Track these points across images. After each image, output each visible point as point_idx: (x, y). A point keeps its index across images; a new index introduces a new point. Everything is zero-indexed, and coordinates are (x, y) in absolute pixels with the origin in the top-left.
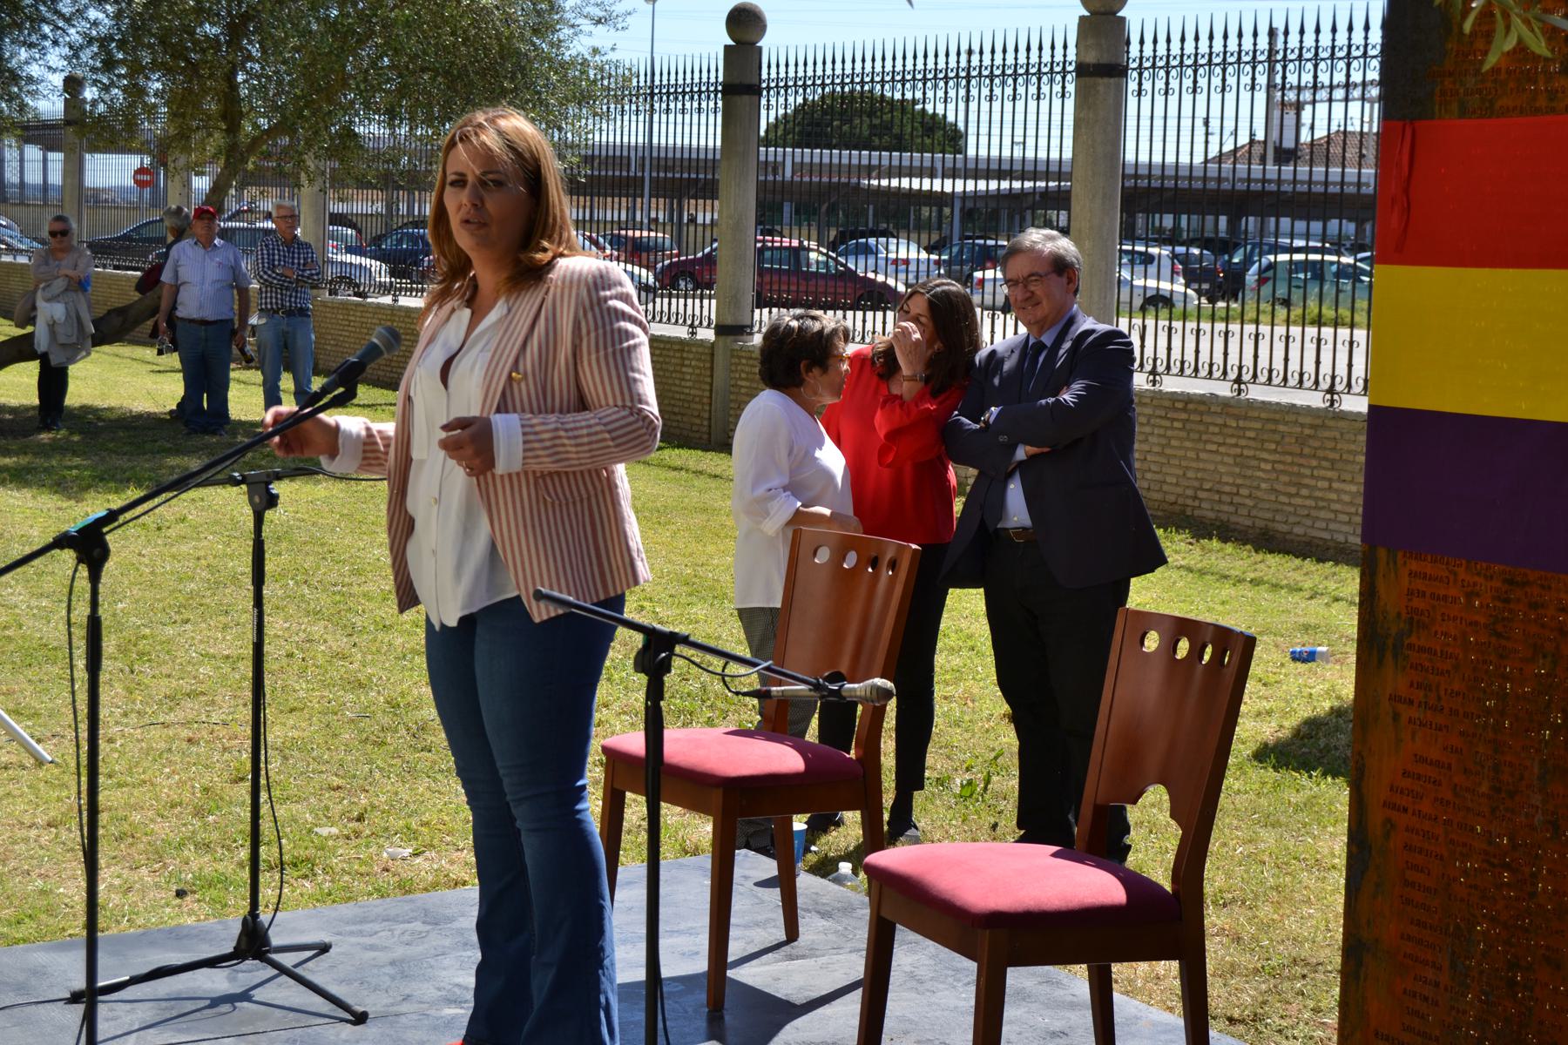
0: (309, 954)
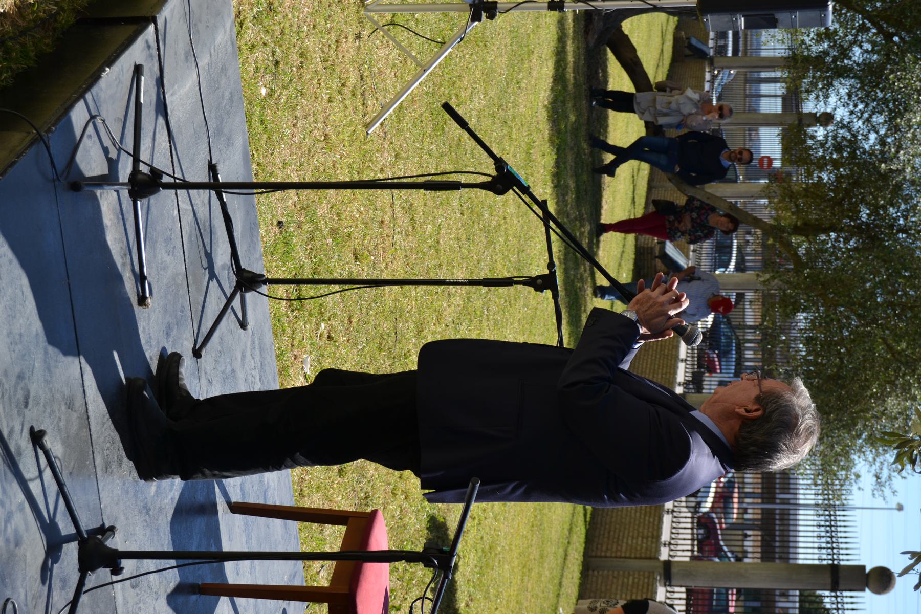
0: (240, 315)
